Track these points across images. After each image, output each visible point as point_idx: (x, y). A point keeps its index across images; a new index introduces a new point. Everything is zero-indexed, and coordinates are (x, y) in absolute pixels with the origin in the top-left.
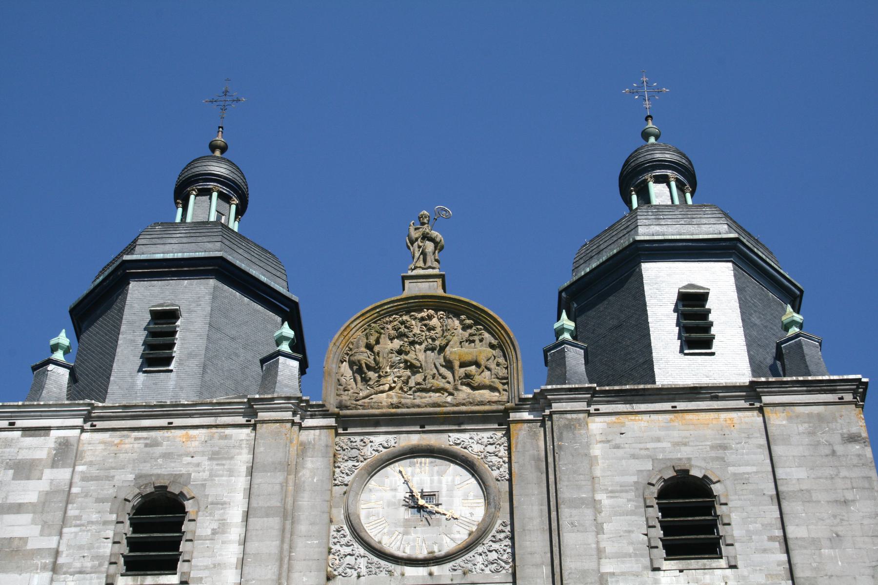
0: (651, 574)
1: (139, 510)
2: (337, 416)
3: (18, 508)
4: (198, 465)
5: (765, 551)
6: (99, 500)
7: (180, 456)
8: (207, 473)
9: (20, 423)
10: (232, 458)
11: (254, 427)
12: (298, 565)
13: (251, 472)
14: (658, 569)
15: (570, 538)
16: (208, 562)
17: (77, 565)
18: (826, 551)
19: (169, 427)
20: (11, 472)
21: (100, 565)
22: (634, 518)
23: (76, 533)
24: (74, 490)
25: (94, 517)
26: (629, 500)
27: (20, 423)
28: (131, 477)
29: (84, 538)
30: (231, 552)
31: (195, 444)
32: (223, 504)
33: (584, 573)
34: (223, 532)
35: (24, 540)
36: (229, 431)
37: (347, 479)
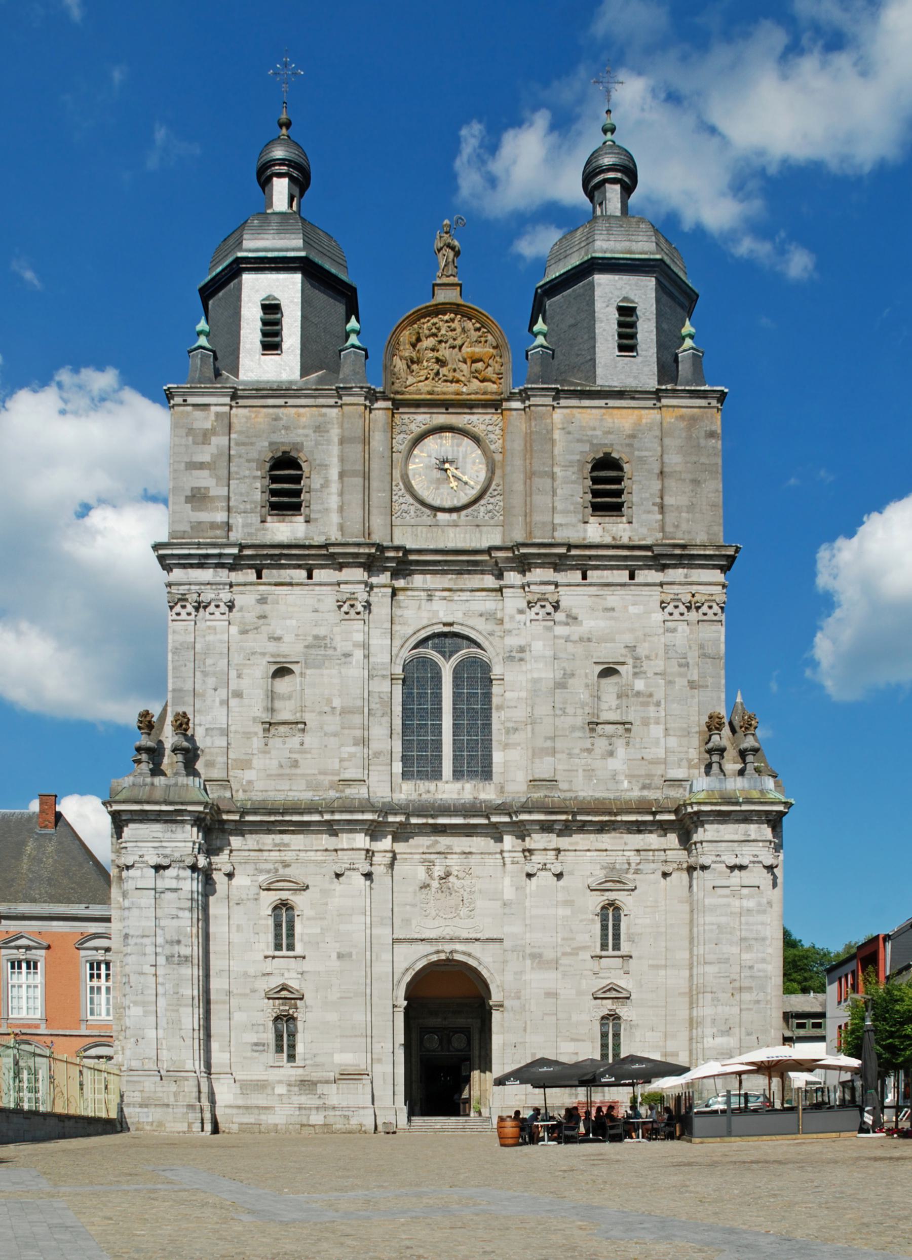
0: (583, 525)
1: (272, 468)
2: (394, 401)
3: (201, 466)
4: (307, 436)
5: (649, 512)
6: (248, 461)
7: (295, 428)
8: (313, 443)
9: (191, 400)
10: (328, 431)
11: (341, 406)
12: (374, 511)
13: (342, 442)
14: (587, 522)
15: (538, 499)
16: (319, 507)
17: (242, 507)
18: (684, 515)
19: (285, 406)
20: (190, 438)
21: (256, 507)
22: (576, 486)
23: (237, 484)
24: (232, 452)
25: (247, 473)
26: (574, 473)
27: (191, 400)
28: (266, 444)
29: (243, 488)
30: (333, 501)
31: (304, 419)
32: (326, 466)
33: (544, 524)
34: (327, 487)
35: (207, 489)
36: (324, 410)
37: (401, 448)
